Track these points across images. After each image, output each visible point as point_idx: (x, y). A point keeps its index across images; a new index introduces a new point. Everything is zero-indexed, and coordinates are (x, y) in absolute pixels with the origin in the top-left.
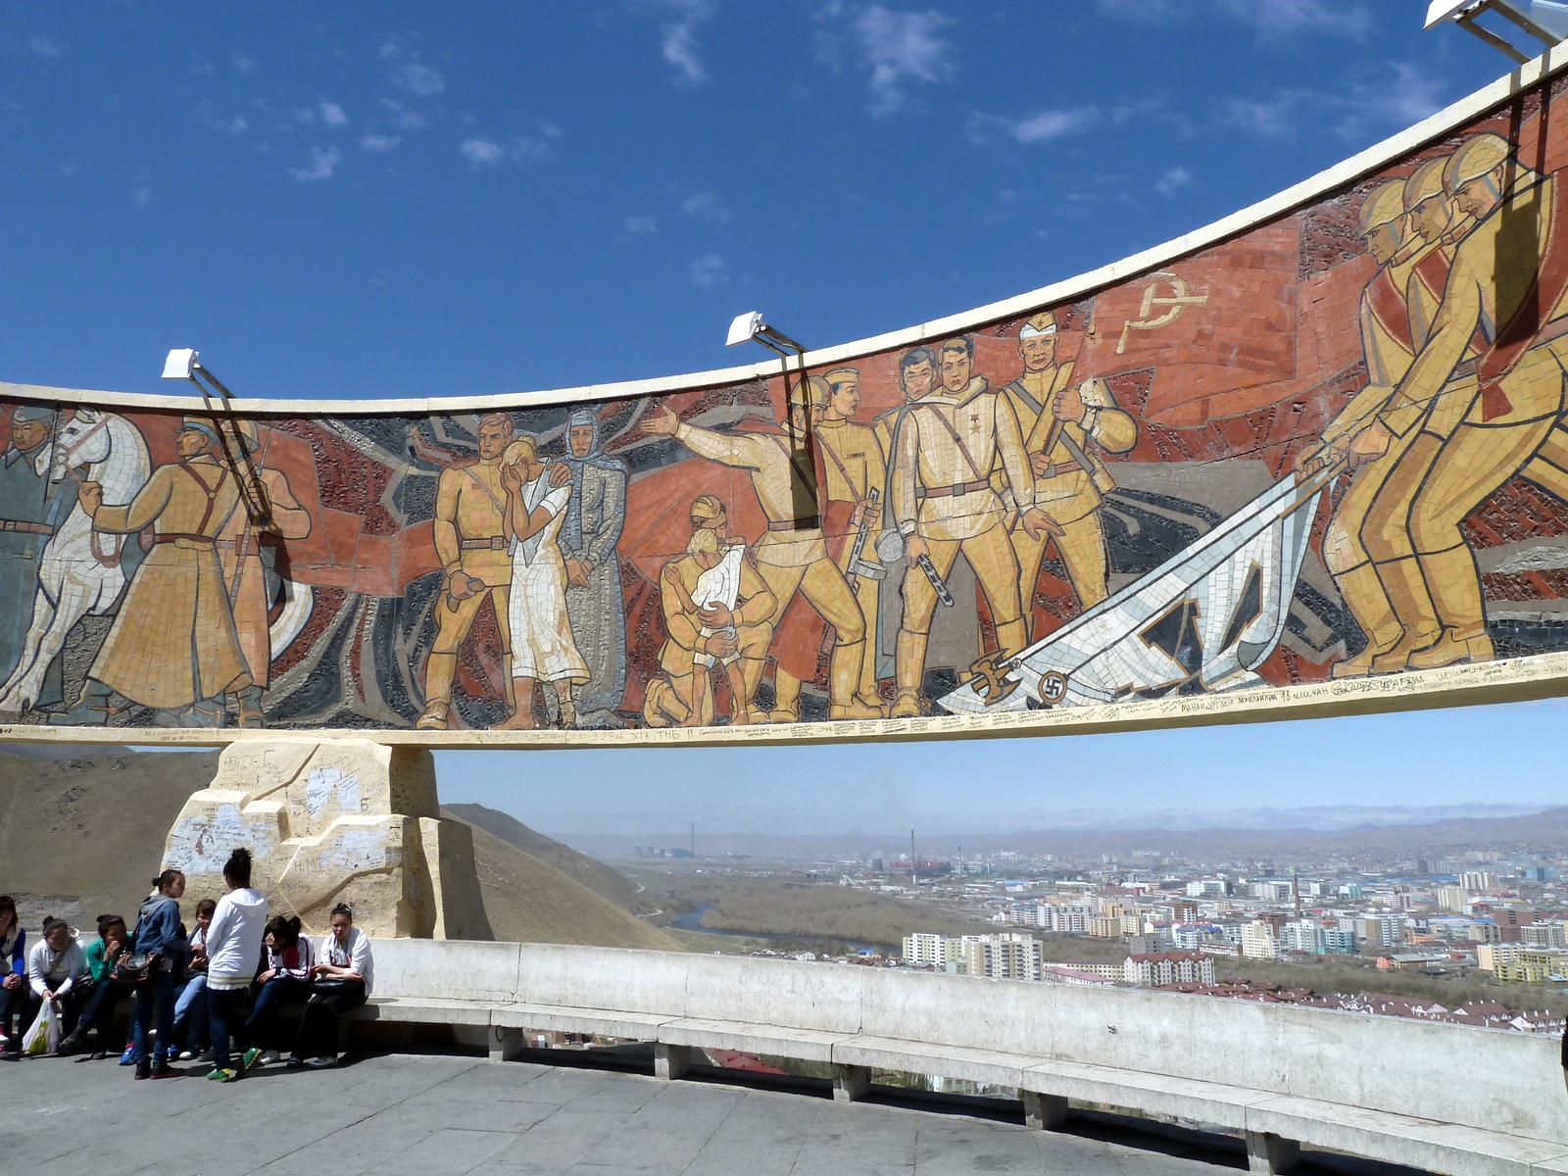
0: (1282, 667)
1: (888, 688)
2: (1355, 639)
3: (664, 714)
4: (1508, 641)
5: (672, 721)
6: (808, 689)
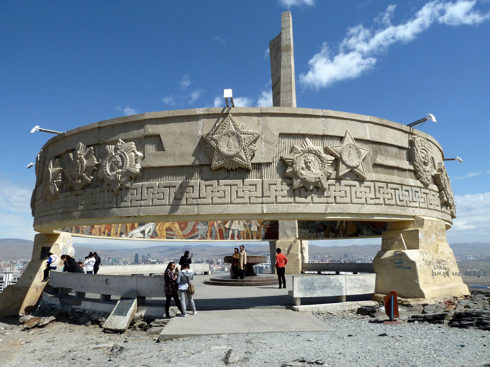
0: (151, 237)
1: (116, 233)
2: (157, 236)
3: (94, 234)
4: (167, 238)
5: (95, 235)
6: (109, 232)
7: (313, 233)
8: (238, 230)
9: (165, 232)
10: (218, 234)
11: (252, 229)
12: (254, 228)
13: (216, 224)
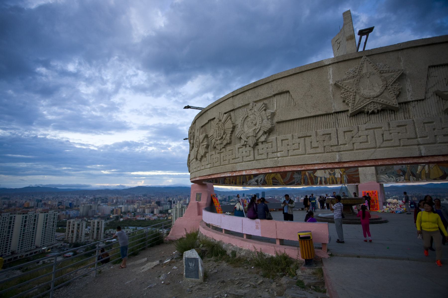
1: (240, 182)
7: (393, 177)
8: (324, 177)
9: (271, 181)
10: (310, 181)
11: (336, 176)
12: (338, 175)
13: (307, 174)
